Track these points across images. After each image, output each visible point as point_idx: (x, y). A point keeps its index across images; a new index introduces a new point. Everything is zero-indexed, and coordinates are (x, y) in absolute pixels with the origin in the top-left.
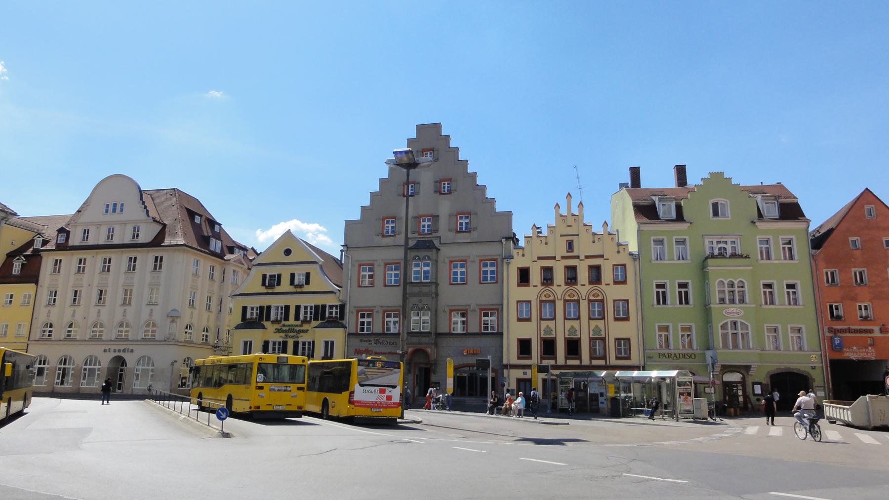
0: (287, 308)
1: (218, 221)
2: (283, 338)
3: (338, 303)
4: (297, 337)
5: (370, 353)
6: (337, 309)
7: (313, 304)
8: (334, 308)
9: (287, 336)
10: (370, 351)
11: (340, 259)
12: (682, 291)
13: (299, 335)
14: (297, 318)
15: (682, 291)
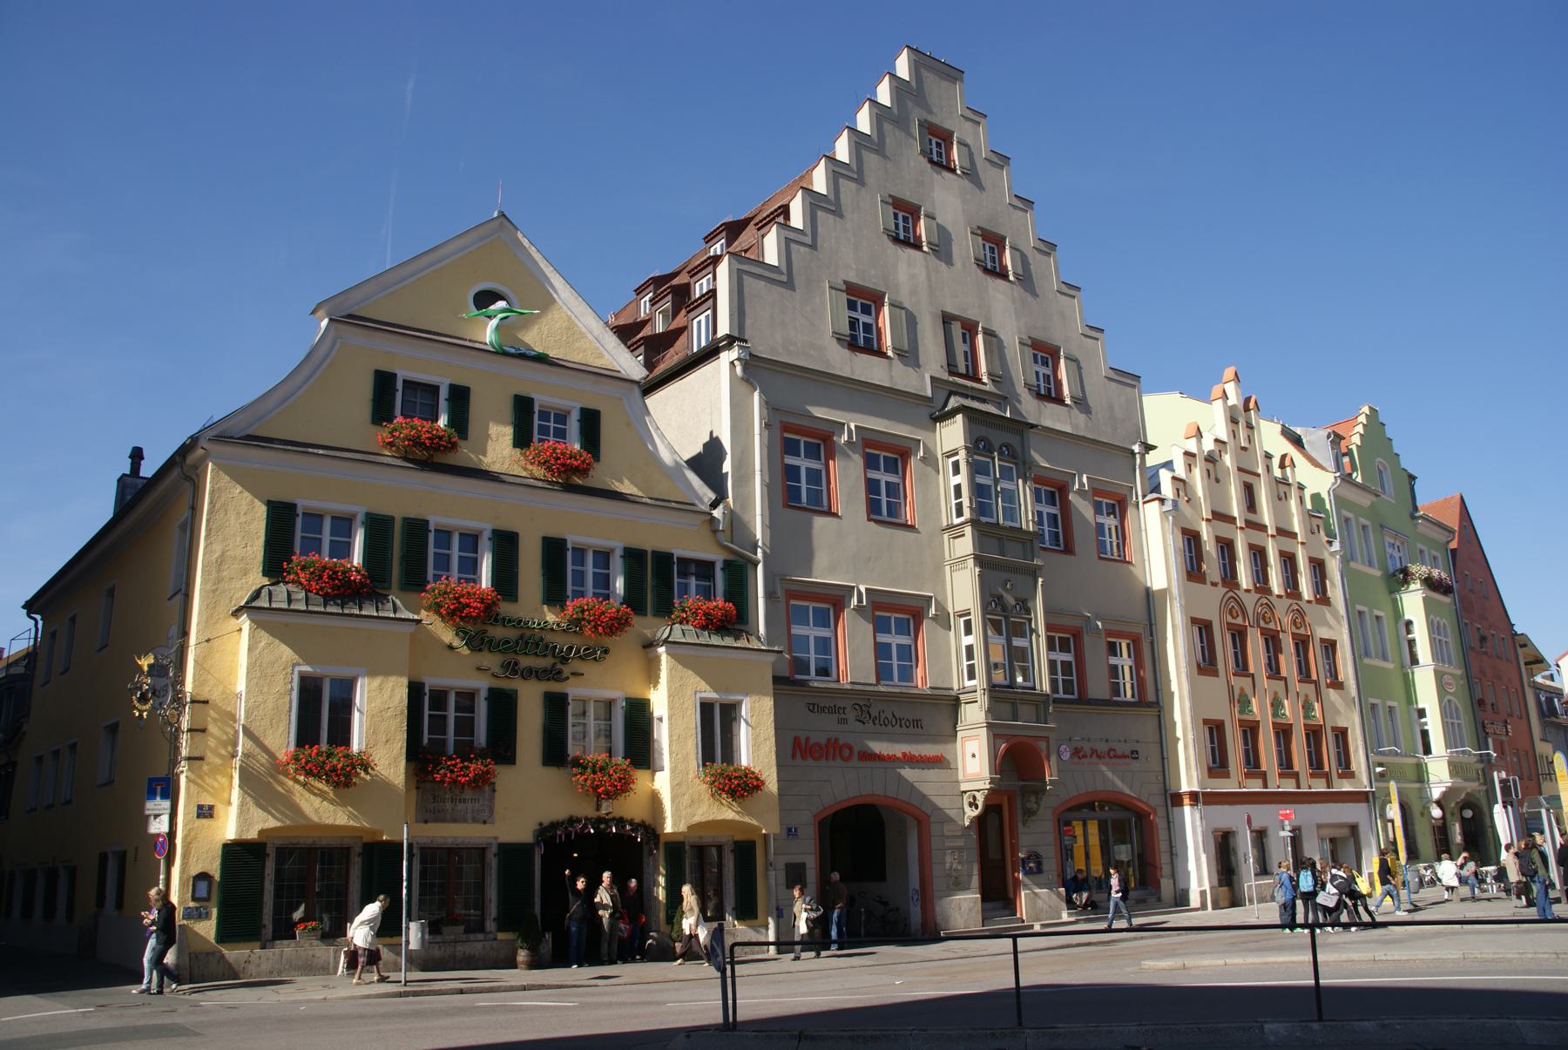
0: (506, 544)
4: (554, 674)
5: (846, 752)
9: (511, 669)
12: (1054, 637)
15: (1054, 637)
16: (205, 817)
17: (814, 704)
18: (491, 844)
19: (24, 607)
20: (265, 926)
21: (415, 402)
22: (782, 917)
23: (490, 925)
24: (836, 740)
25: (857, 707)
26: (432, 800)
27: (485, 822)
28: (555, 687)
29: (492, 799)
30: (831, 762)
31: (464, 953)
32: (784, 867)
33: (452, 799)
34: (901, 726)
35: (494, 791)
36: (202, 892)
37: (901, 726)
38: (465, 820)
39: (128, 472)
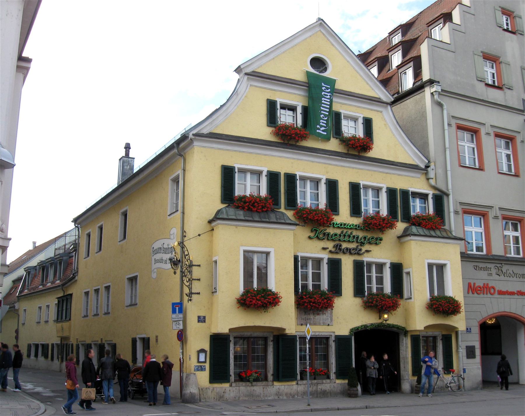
2: (331, 252)
4: (358, 252)
5: (492, 291)
9: (338, 249)
10: (493, 288)
14: (355, 210)
16: (202, 322)
17: (477, 266)
19: (72, 222)
20: (231, 375)
21: (286, 115)
22: (465, 372)
23: (333, 376)
24: (487, 284)
25: (496, 267)
27: (329, 325)
29: (332, 313)
30: (485, 296)
31: (321, 389)
32: (465, 348)
34: (516, 277)
36: (202, 358)
37: (516, 277)
39: (124, 155)
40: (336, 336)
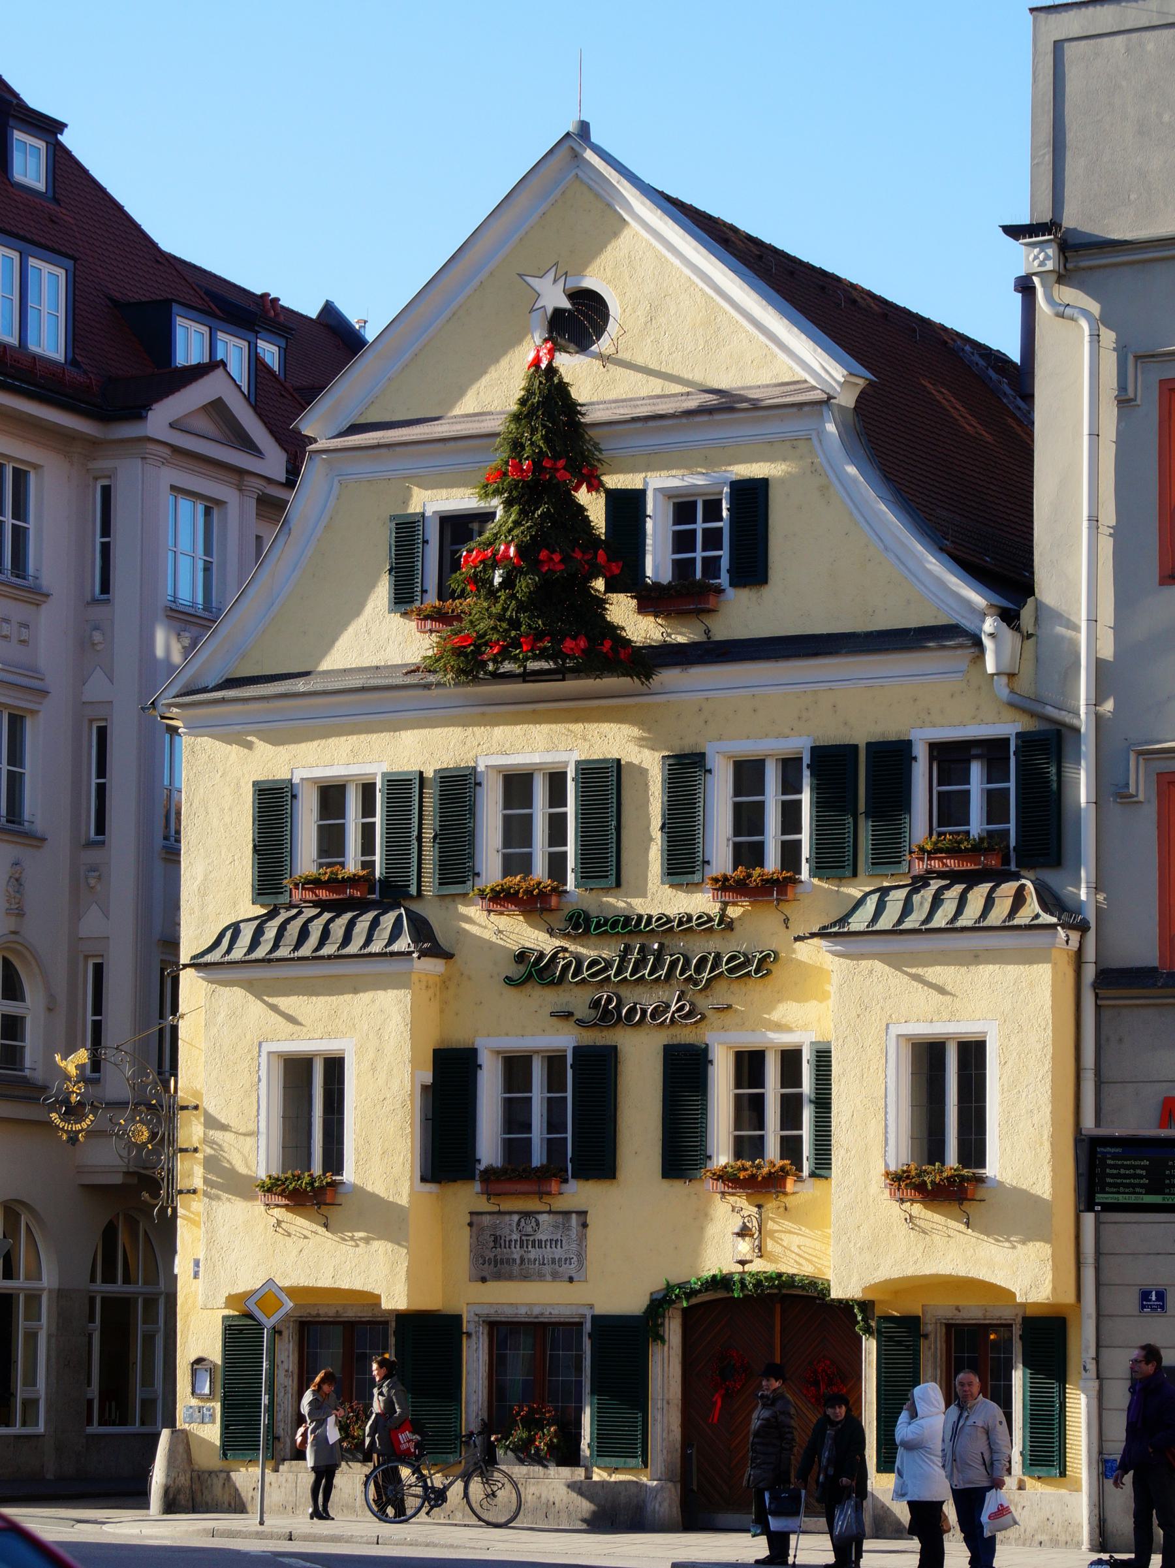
1: (36, 98)
2: (580, 1023)
3: (1008, 727)
6: (996, 770)
7: (800, 744)
8: (976, 770)
11: (1015, 356)
13: (705, 1003)
18: (584, 1316)
26: (492, 1244)
27: (571, 1280)
28: (685, 1035)
29: (582, 1238)
33: (522, 1241)
35: (585, 1225)
38: (541, 1277)
40: (595, 1318)
